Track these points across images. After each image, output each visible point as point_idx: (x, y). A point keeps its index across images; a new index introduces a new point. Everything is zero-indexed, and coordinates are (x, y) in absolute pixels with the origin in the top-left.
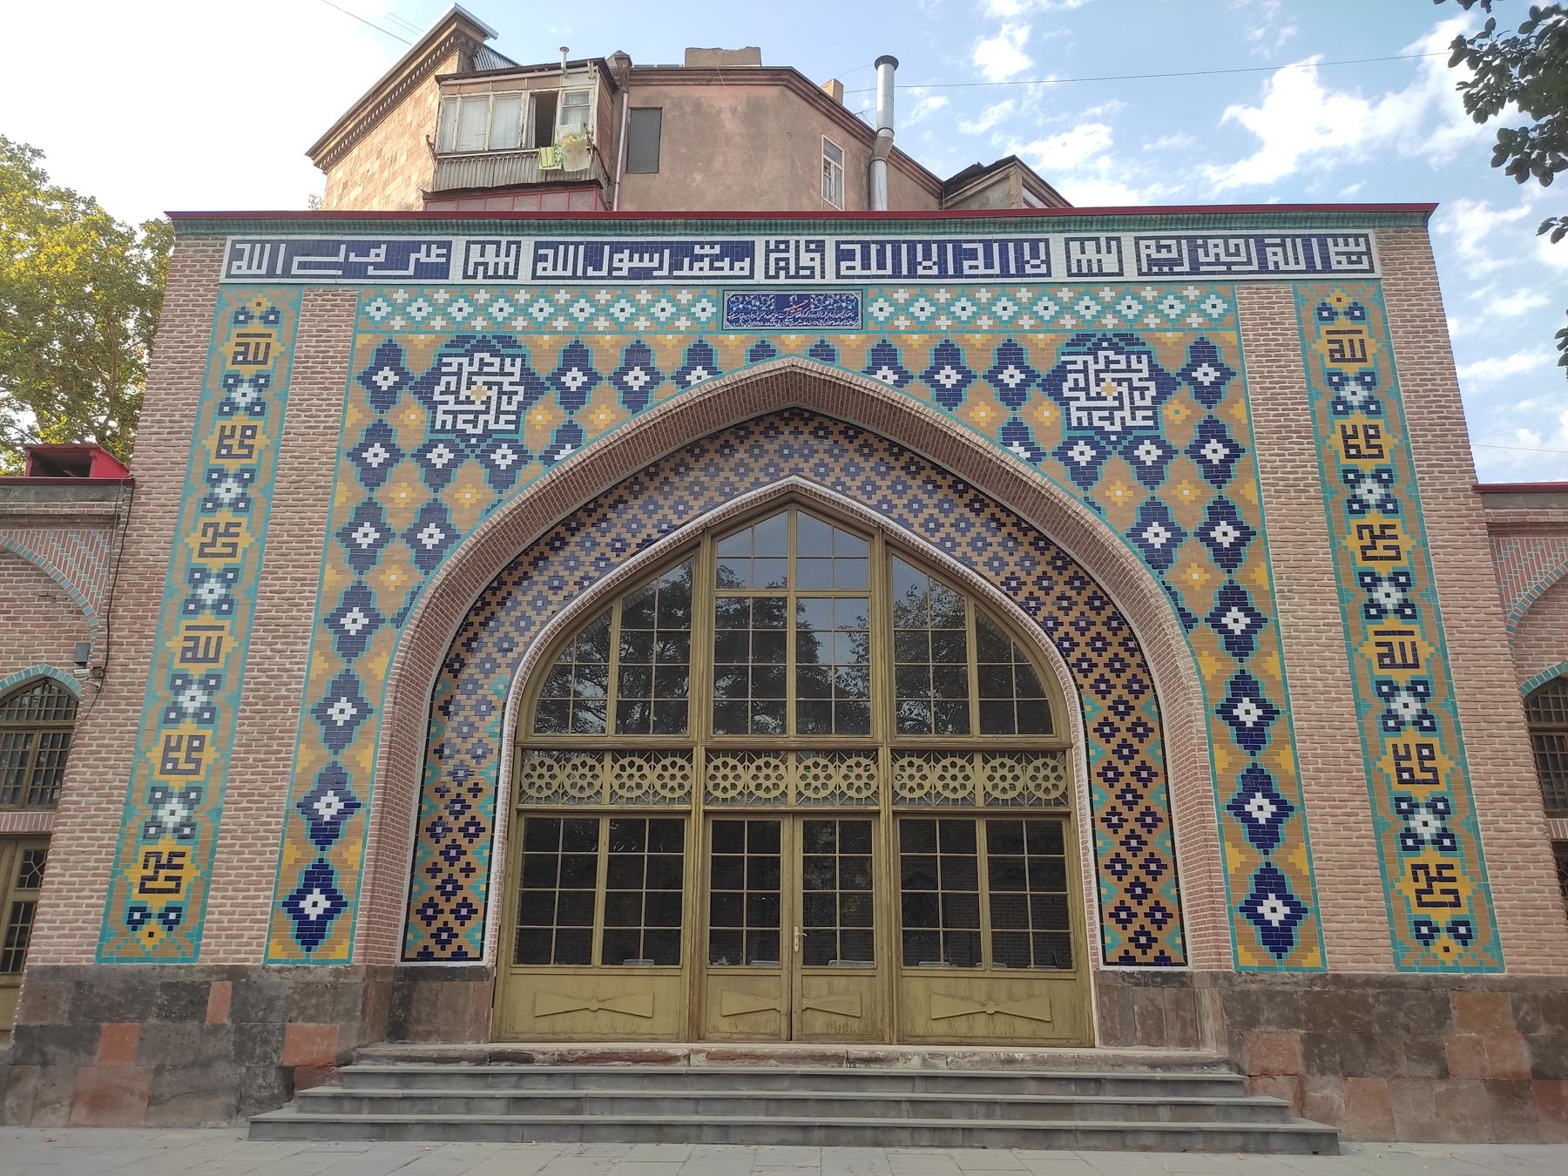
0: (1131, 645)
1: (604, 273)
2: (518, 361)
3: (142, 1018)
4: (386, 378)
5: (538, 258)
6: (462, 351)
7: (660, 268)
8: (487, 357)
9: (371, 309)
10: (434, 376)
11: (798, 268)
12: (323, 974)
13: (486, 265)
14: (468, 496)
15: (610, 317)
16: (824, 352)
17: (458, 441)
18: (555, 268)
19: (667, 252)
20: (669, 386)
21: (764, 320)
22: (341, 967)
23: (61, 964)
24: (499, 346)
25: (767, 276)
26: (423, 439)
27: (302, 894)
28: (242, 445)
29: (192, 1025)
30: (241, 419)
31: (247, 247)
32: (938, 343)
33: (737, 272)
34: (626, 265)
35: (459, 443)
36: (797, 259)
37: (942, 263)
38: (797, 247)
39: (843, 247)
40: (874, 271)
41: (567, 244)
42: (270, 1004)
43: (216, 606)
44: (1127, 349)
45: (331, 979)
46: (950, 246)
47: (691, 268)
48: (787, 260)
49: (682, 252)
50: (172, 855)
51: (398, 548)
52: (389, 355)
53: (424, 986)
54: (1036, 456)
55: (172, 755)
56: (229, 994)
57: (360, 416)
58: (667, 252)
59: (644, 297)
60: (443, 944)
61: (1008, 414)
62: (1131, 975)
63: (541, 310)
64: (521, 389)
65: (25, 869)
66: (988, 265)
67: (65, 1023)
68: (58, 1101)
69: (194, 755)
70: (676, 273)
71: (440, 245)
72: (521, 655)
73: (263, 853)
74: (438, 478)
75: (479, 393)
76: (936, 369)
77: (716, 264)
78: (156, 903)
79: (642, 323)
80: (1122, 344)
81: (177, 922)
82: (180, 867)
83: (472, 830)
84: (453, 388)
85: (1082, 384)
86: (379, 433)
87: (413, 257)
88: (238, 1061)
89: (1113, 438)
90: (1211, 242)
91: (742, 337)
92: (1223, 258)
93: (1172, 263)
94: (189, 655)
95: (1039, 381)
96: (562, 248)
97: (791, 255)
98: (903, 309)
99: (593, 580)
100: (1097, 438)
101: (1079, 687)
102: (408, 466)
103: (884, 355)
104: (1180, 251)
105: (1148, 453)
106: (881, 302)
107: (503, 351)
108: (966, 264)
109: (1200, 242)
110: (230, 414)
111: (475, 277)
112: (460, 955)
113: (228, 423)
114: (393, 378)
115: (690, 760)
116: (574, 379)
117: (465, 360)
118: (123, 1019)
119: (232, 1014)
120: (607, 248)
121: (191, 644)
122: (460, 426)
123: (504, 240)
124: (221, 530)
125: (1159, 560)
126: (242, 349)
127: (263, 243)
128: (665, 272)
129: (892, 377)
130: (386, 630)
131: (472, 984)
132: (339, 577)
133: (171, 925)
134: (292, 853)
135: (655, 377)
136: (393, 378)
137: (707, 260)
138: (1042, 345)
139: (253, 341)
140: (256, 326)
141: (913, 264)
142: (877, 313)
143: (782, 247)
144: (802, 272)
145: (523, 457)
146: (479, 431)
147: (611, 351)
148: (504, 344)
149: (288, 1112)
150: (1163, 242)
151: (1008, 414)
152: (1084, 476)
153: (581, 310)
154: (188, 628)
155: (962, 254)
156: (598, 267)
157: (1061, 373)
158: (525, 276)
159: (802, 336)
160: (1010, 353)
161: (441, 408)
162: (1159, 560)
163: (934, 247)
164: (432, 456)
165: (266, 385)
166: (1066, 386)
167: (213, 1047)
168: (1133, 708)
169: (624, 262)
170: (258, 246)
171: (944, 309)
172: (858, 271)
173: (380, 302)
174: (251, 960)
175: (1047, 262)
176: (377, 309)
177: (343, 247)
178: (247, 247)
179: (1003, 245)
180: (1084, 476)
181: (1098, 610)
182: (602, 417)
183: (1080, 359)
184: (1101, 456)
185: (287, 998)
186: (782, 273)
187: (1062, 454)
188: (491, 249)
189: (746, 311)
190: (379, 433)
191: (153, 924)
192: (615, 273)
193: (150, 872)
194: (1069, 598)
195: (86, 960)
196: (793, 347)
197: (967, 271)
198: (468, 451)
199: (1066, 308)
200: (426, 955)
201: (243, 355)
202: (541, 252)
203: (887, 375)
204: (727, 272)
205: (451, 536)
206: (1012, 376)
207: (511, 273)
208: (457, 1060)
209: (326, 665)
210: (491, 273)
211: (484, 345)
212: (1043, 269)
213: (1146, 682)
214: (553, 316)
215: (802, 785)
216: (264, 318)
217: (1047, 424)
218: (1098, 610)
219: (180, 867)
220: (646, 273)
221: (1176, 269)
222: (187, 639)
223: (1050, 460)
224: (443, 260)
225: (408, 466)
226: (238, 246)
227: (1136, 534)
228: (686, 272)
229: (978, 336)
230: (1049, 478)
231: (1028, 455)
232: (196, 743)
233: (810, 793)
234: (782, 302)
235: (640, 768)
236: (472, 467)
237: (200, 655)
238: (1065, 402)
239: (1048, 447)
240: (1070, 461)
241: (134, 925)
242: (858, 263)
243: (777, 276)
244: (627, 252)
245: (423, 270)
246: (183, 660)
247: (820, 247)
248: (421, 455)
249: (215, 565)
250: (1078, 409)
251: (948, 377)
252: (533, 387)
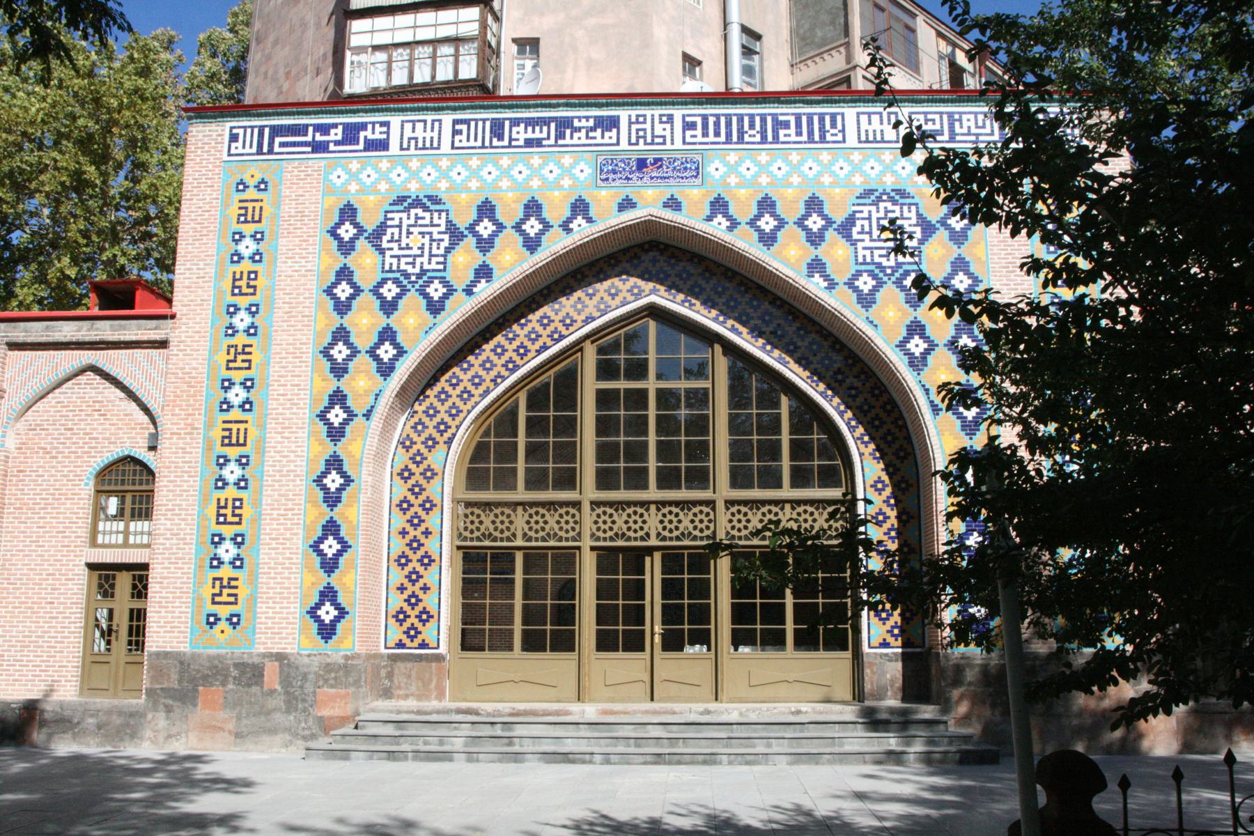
0: (900, 423)
1: (506, 143)
2: (444, 215)
3: (224, 684)
4: (347, 231)
5: (455, 133)
6: (401, 208)
7: (548, 138)
8: (419, 211)
9: (333, 177)
10: (381, 229)
11: (653, 137)
12: (338, 658)
13: (416, 139)
14: (411, 321)
15: (511, 178)
16: (673, 204)
17: (402, 279)
18: (468, 140)
19: (553, 125)
20: (556, 230)
21: (628, 179)
22: (349, 653)
23: (168, 649)
24: (428, 204)
25: (630, 144)
26: (379, 276)
27: (318, 606)
28: (249, 286)
29: (255, 689)
30: (246, 266)
31: (241, 131)
32: (760, 196)
33: (606, 141)
34: (522, 137)
35: (402, 280)
36: (653, 129)
38: (653, 120)
39: (688, 119)
40: (711, 138)
41: (476, 120)
42: (305, 677)
43: (242, 406)
44: (901, 201)
45: (342, 661)
46: (769, 119)
47: (572, 137)
48: (644, 130)
49: (564, 125)
50: (230, 579)
51: (363, 360)
52: (348, 213)
53: (401, 667)
54: (832, 285)
55: (222, 511)
56: (278, 670)
57: (330, 261)
58: (553, 125)
59: (536, 161)
60: (412, 638)
61: (812, 252)
62: (886, 655)
63: (459, 174)
64: (446, 237)
65: (134, 587)
66: (799, 134)
67: (176, 686)
68: (179, 734)
69: (237, 511)
70: (560, 142)
71: (382, 124)
72: (454, 435)
73: (289, 578)
74: (389, 307)
75: (415, 241)
76: (758, 217)
77: (591, 134)
78: (224, 611)
79: (535, 183)
80: (897, 197)
81: (238, 623)
82: (236, 587)
83: (426, 561)
84: (396, 237)
85: (867, 229)
86: (344, 274)
88: (288, 712)
89: (889, 271)
90: (965, 117)
91: (613, 191)
92: (974, 130)
94: (226, 441)
95: (835, 226)
96: (473, 124)
97: (648, 126)
98: (733, 169)
99: (504, 378)
100: (877, 271)
101: (861, 455)
102: (366, 298)
103: (719, 206)
104: (942, 124)
106: (717, 164)
107: (433, 207)
108: (782, 132)
109: (957, 117)
110: (238, 262)
111: (408, 149)
112: (423, 645)
113: (237, 268)
114: (353, 231)
115: (579, 510)
116: (486, 228)
117: (404, 215)
118: (212, 685)
119: (281, 683)
120: (507, 123)
121: (227, 433)
122: (403, 267)
123: (429, 117)
124: (240, 350)
125: (917, 363)
126: (243, 212)
127: (252, 127)
128: (552, 141)
129: (726, 223)
130: (359, 420)
131: (434, 664)
132: (323, 384)
133: (234, 625)
134: (310, 579)
135: (547, 226)
136: (353, 231)
137: (584, 131)
138: (838, 198)
139: (250, 205)
140: (251, 193)
141: (741, 133)
142: (713, 172)
143: (641, 119)
144: (657, 140)
145: (450, 291)
146: (417, 270)
147: (513, 206)
149: (323, 742)
150: (929, 117)
151: (812, 252)
152: (866, 301)
153: (490, 172)
154: (225, 422)
155: (780, 125)
156: (501, 138)
157: (851, 220)
159: (657, 191)
160: (814, 205)
161: (388, 253)
162: (917, 363)
163: (758, 119)
164: (383, 291)
165: (262, 239)
166: (855, 230)
167: (272, 703)
168: (899, 470)
169: (521, 134)
170: (249, 131)
171: (764, 168)
172: (700, 139)
173: (339, 171)
174: (290, 649)
175: (843, 131)
176: (338, 177)
177: (311, 129)
178: (241, 131)
179: (810, 118)
180: (866, 301)
181: (877, 397)
182: (508, 257)
183: (866, 209)
184: (880, 284)
185: (316, 673)
186: (641, 141)
187: (850, 284)
188: (420, 126)
189: (614, 172)
190: (344, 274)
191: (223, 625)
192: (514, 143)
193: (217, 591)
194: (856, 388)
195: (185, 648)
196: (650, 200)
197: (782, 139)
198: (409, 286)
199: (857, 169)
200: (400, 645)
201: (244, 218)
202: (458, 127)
203: (720, 223)
204: (599, 141)
205: (401, 352)
206: (815, 223)
207: (435, 145)
208: (430, 713)
209: (320, 448)
210: (420, 145)
211: (417, 203)
212: (840, 137)
213: (910, 450)
214: (468, 179)
215: (660, 527)
216: (257, 187)
217: (840, 260)
218: (877, 397)
219: (236, 587)
220: (538, 143)
221: (938, 138)
222: (224, 430)
223: (842, 288)
224: (385, 136)
225: (366, 298)
226: (235, 131)
227: (902, 345)
228: (568, 141)
229: (790, 191)
230: (840, 303)
231: (826, 284)
232: (238, 504)
233: (666, 533)
234: (642, 164)
235: (543, 516)
236: (413, 300)
237: (234, 441)
238: (854, 243)
239: (841, 278)
240: (856, 289)
241: (211, 625)
242: (699, 132)
243: (637, 144)
244: (522, 125)
245: (372, 145)
246: (223, 445)
247: (670, 118)
248: (376, 291)
249: (238, 376)
250: (864, 248)
251: (768, 223)
252: (455, 235)
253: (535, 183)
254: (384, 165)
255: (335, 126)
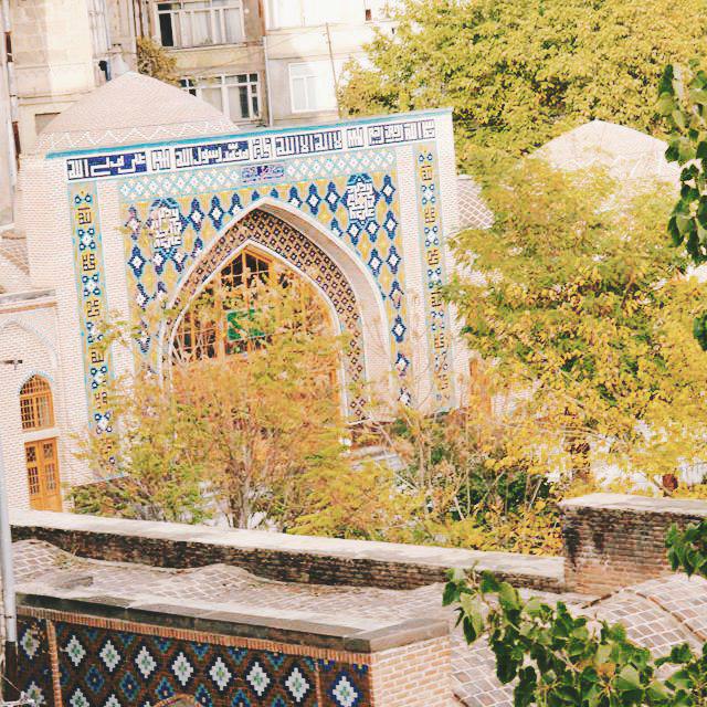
37: (309, 146)
87: (133, 161)
93: (379, 138)
105: (372, 228)
148: (169, 203)
158: (173, 168)
162: (375, 272)
169: (206, 155)
177: (108, 159)
189: (248, 176)
220: (212, 161)
226: (70, 163)
253: (215, 186)
254: (146, 181)
255: (119, 156)
